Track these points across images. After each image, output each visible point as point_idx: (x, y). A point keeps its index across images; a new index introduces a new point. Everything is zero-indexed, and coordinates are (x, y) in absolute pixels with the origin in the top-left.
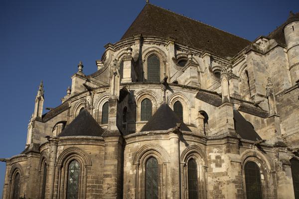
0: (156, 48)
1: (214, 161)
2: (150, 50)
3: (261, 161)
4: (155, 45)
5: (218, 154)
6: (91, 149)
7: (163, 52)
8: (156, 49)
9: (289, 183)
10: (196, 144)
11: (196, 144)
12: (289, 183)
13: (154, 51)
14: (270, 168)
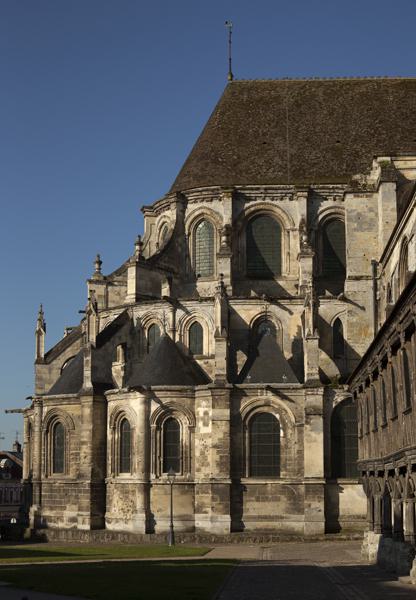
0: (205, 208)
1: (202, 419)
2: (197, 213)
3: (280, 410)
4: (205, 204)
5: (206, 409)
6: (72, 409)
7: (217, 213)
8: (205, 211)
9: (315, 441)
10: (175, 399)
11: (175, 399)
12: (315, 441)
13: (203, 214)
14: (293, 420)
